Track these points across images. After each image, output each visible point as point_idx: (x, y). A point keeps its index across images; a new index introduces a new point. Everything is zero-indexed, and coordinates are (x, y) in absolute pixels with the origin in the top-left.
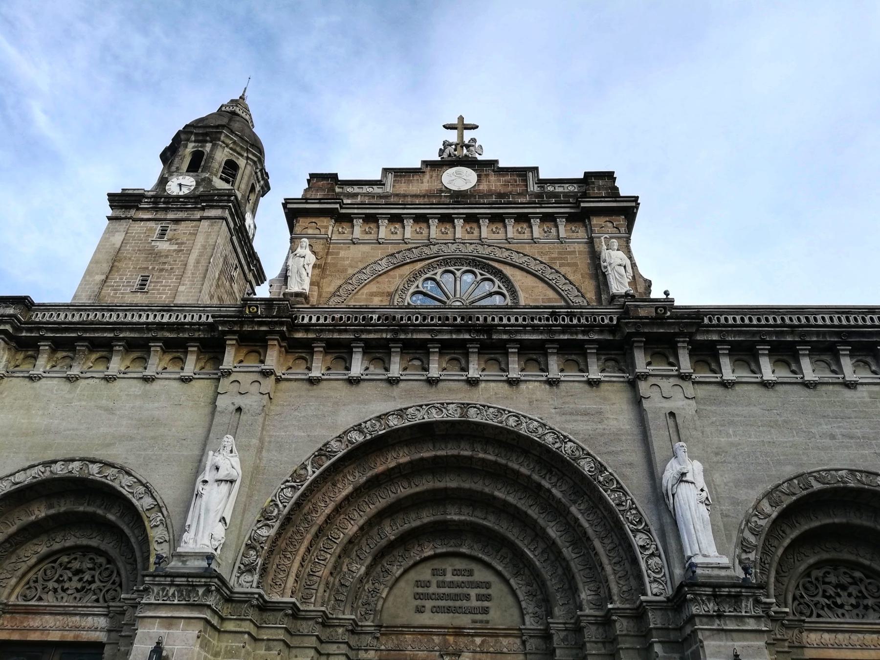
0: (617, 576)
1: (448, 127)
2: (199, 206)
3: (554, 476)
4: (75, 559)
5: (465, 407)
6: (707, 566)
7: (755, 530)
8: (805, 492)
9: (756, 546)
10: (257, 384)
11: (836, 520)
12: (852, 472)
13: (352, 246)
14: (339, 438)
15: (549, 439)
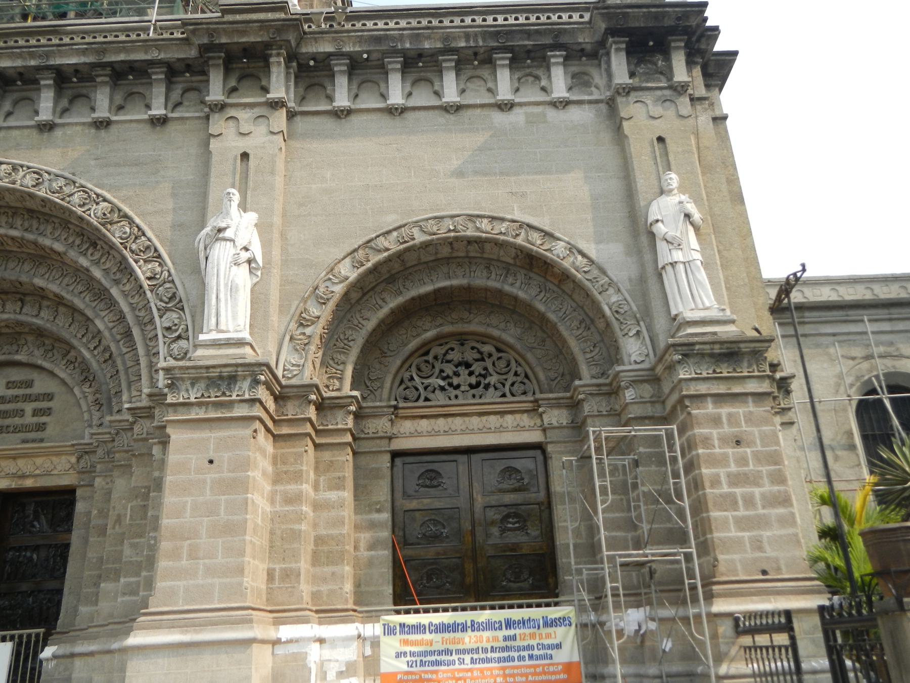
0: (153, 370)
3: (99, 250)
6: (215, 344)
7: (322, 298)
8: (402, 247)
9: (318, 317)
11: (455, 282)
12: (471, 217)
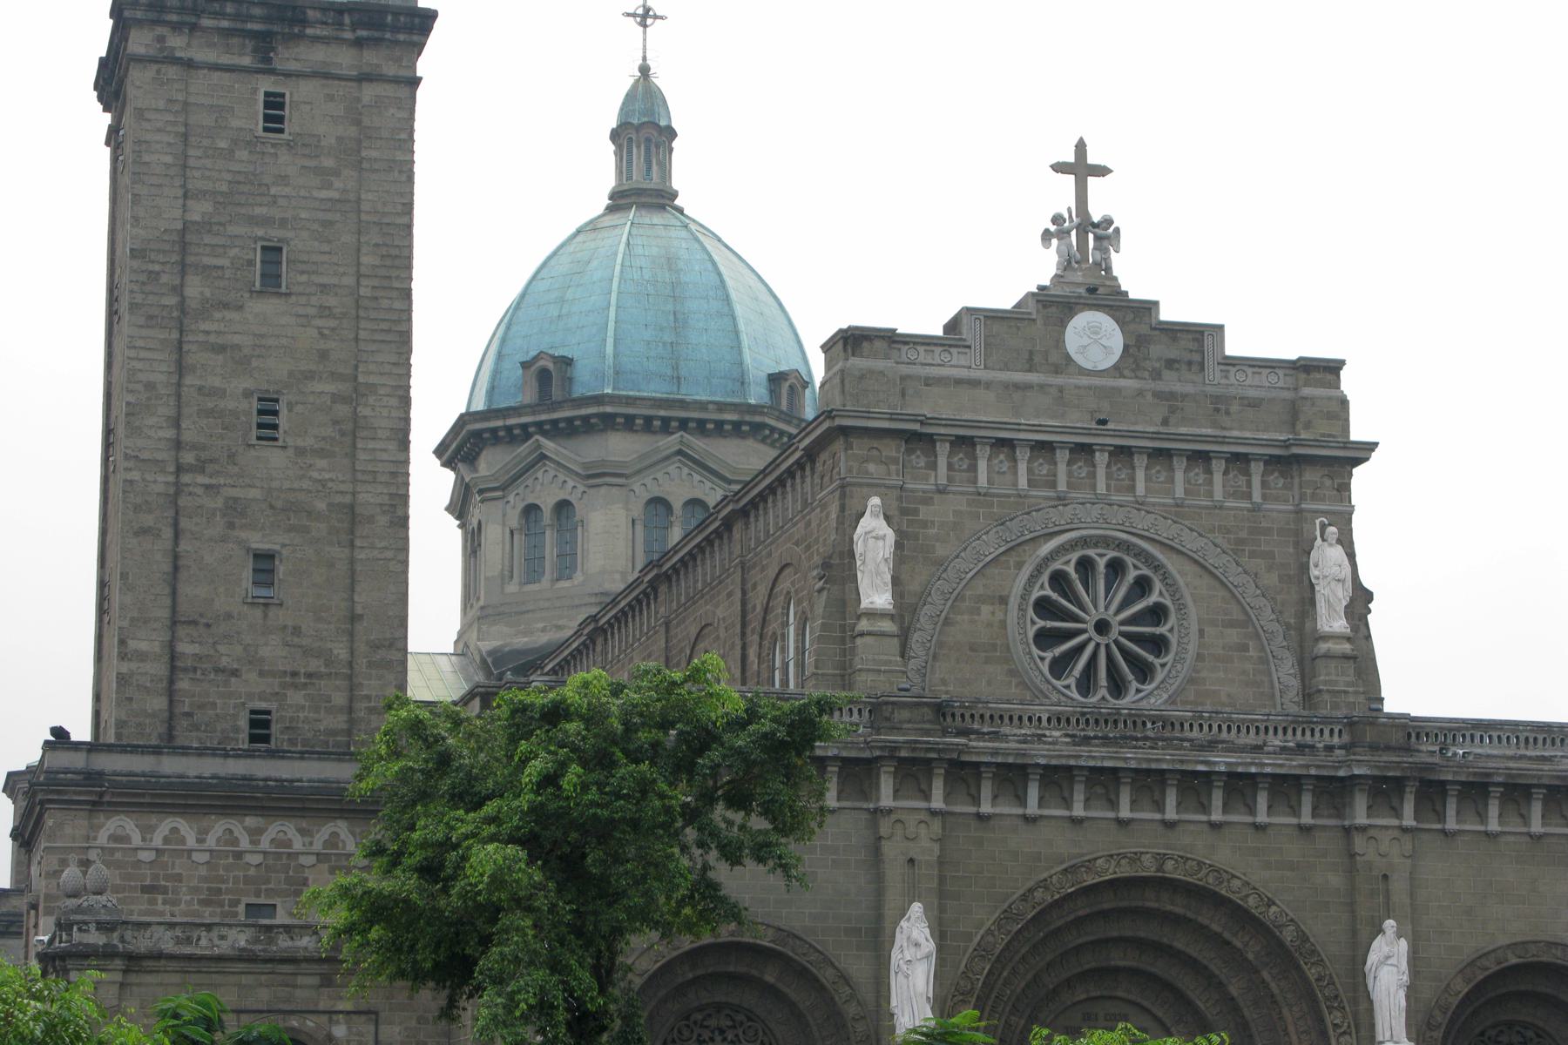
1: (1059, 168)
2: (348, 35)
4: (710, 1015)
5: (1161, 859)
8: (1498, 968)
9: (1441, 1024)
10: (923, 825)
12: (1551, 945)
13: (936, 497)
14: (1024, 898)
15: (1252, 901)
